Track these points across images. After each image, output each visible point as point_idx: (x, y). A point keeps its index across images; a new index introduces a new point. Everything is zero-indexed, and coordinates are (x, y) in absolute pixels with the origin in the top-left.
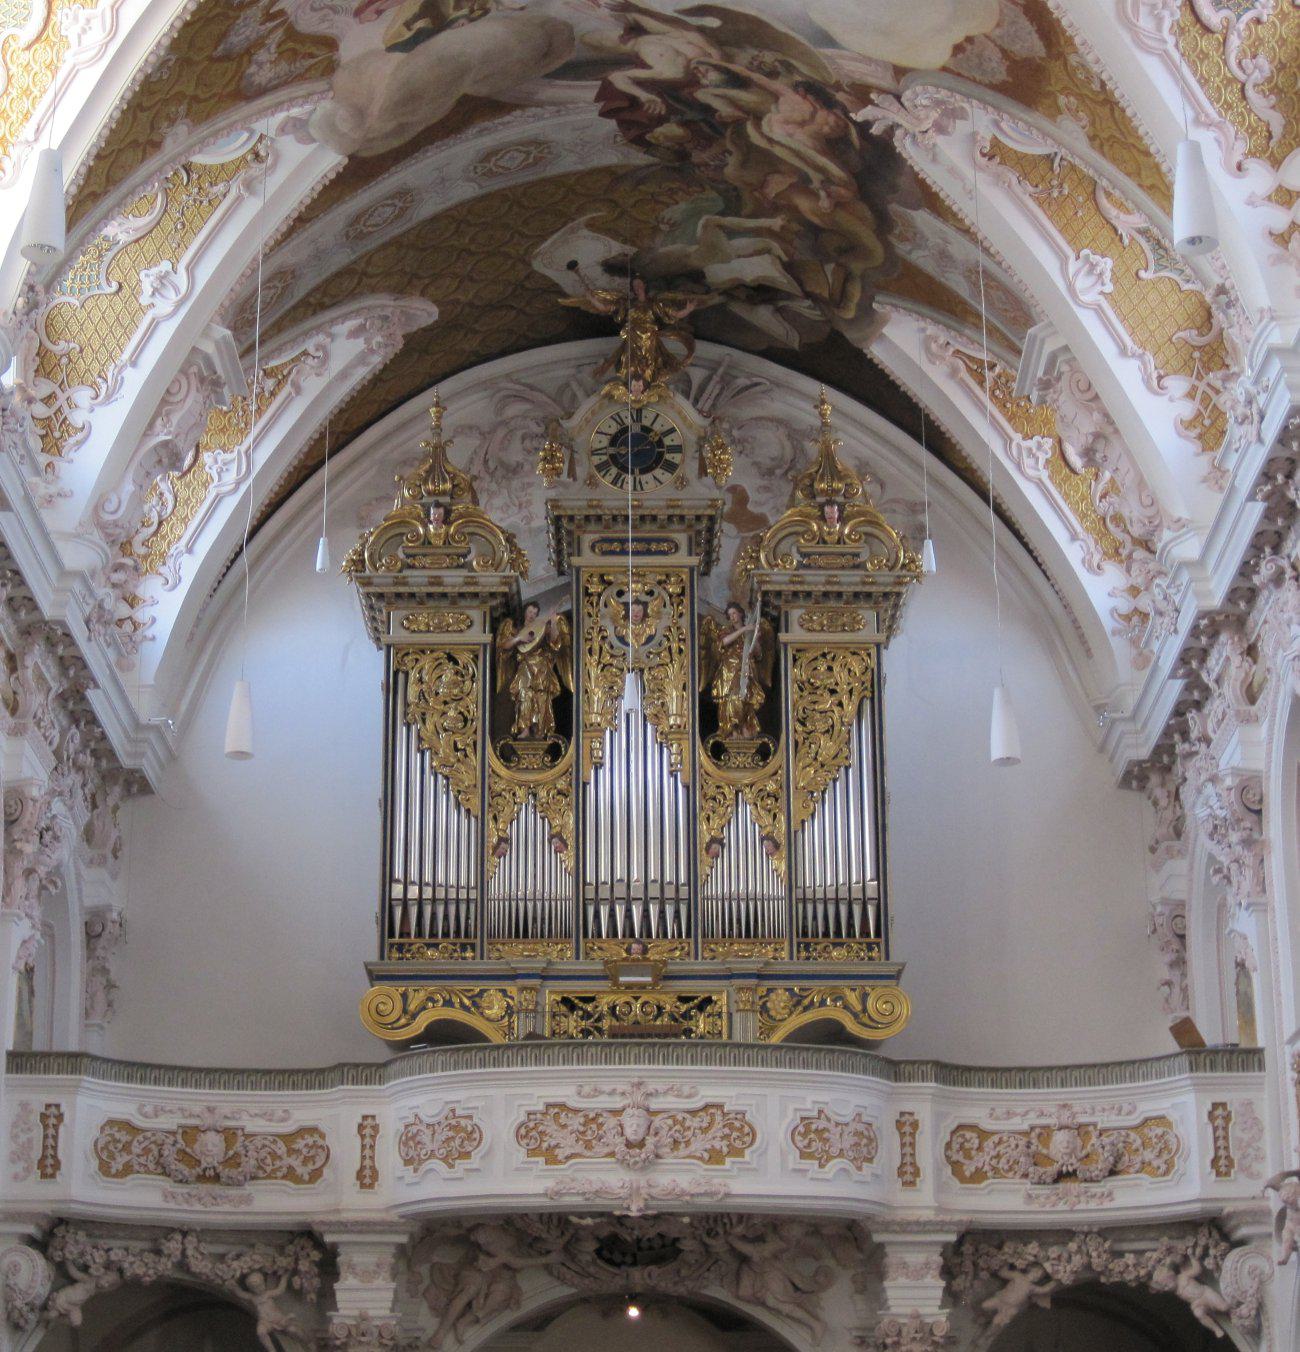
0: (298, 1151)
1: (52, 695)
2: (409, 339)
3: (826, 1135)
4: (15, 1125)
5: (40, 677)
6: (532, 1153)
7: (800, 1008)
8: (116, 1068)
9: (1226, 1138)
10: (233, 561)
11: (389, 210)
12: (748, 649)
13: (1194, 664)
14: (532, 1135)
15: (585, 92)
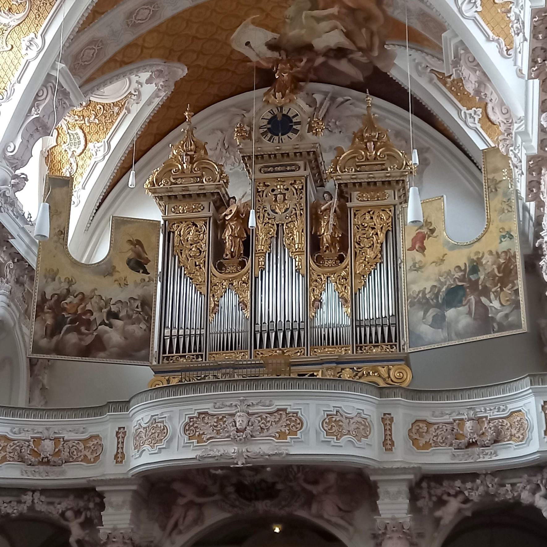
0: (90, 447)
2: (176, 83)
3: (341, 423)
7: (357, 377)
12: (332, 211)
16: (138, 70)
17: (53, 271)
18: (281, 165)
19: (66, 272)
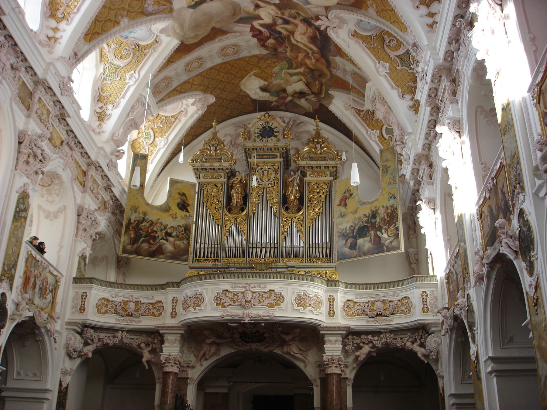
0: (156, 308)
2: (208, 106)
3: (306, 300)
4: (74, 298)
5: (95, 181)
6: (218, 304)
8: (104, 283)
9: (426, 302)
11: (197, 63)
13: (415, 174)
14: (219, 300)
15: (247, 28)
16: (188, 97)
17: (135, 206)
18: (267, 155)
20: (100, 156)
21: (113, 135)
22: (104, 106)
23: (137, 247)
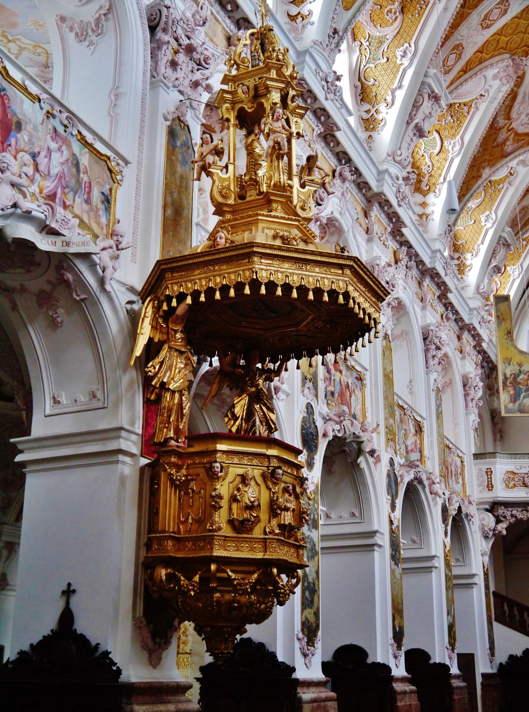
1: (472, 346)
4: (478, 476)
5: (468, 341)
8: (507, 455)
10: (521, 299)
17: (508, 358)
19: (516, 359)
20: (474, 317)
21: (478, 288)
22: (461, 256)
23: (520, 405)
